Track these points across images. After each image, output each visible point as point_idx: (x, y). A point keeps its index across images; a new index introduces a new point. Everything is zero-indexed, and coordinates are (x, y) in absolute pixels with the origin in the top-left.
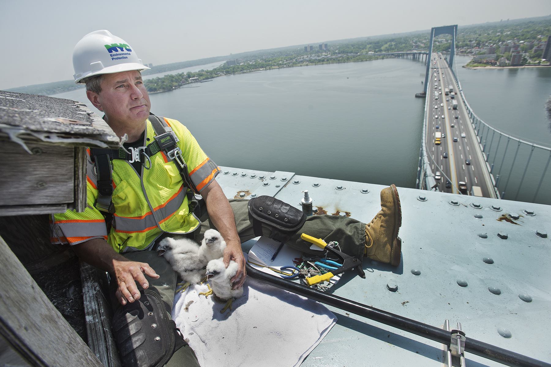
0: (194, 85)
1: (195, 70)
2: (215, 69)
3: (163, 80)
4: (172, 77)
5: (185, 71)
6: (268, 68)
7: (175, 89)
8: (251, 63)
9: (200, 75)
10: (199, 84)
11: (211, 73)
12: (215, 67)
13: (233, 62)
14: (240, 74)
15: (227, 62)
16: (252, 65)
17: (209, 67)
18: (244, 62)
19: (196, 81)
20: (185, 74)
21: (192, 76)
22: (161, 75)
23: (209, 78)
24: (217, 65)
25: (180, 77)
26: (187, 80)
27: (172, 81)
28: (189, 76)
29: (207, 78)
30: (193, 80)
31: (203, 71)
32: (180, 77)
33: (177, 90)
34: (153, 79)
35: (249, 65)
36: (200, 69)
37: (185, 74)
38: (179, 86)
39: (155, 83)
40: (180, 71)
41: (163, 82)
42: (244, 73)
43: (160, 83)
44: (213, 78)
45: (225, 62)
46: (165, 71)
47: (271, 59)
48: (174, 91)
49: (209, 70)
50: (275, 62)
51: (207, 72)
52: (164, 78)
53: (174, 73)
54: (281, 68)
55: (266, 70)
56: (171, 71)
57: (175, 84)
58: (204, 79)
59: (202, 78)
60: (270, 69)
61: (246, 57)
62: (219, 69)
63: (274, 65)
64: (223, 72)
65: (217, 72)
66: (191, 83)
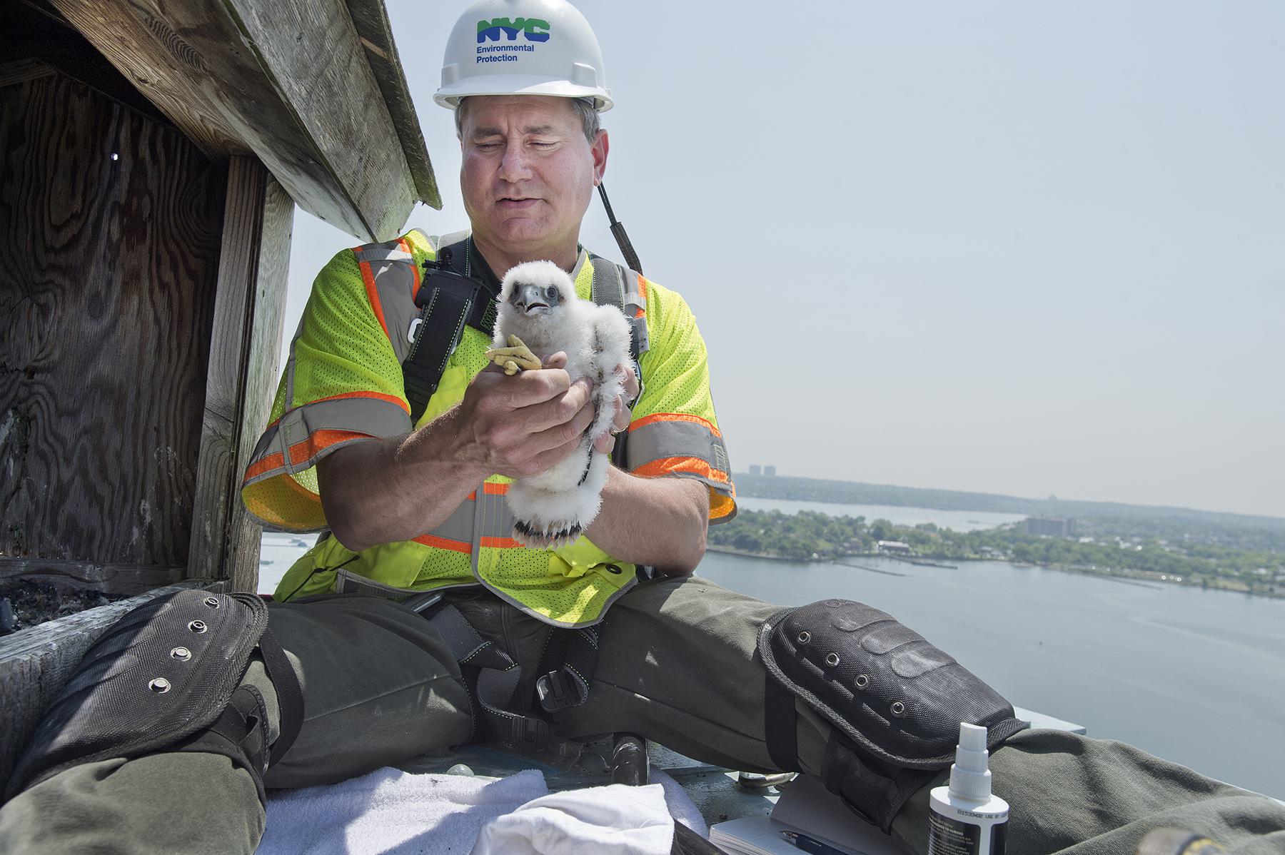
0: (885, 565)
1: (906, 518)
2: (978, 534)
3: (789, 524)
4: (822, 521)
5: (871, 514)
6: (1196, 578)
7: (818, 561)
8: (1123, 545)
9: (918, 537)
10: (904, 568)
11: (959, 540)
12: (981, 528)
13: (1055, 527)
14: (1071, 571)
15: (1031, 521)
16: (1126, 553)
17: (960, 523)
18: (1098, 536)
19: (898, 555)
20: (868, 522)
21: (888, 534)
22: (790, 508)
23: (945, 558)
24: (988, 522)
25: (849, 530)
26: (866, 543)
27: (818, 534)
28: (880, 531)
29: (940, 557)
30: (889, 548)
31: (931, 527)
32: (849, 530)
33: (823, 567)
34: (761, 512)
35: (1117, 550)
36: (925, 522)
37: (868, 522)
38: (838, 557)
39: (764, 525)
40: (854, 511)
41: (789, 529)
42: (1086, 572)
43: (776, 531)
44: (961, 559)
45: (1022, 517)
46: (806, 498)
47: (1215, 550)
48: (814, 568)
49: (955, 529)
50: (1233, 566)
51: (947, 535)
52: (795, 519)
53: (833, 511)
54: (1261, 594)
55: (1185, 584)
56: (824, 501)
57: (824, 545)
58: (925, 556)
59: (920, 549)
60: (1205, 586)
61: (1112, 519)
62: (993, 538)
63: (1227, 576)
64: (1004, 550)
65: (982, 544)
66: (880, 555)
